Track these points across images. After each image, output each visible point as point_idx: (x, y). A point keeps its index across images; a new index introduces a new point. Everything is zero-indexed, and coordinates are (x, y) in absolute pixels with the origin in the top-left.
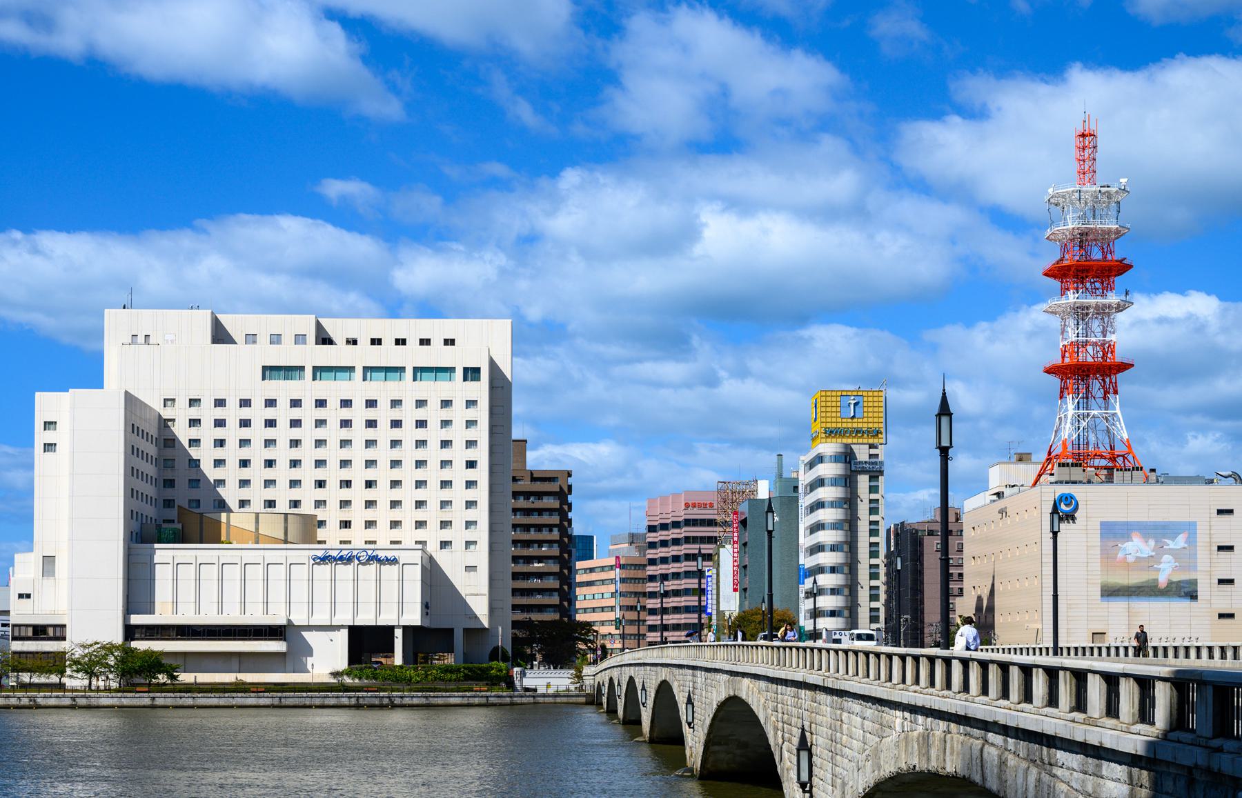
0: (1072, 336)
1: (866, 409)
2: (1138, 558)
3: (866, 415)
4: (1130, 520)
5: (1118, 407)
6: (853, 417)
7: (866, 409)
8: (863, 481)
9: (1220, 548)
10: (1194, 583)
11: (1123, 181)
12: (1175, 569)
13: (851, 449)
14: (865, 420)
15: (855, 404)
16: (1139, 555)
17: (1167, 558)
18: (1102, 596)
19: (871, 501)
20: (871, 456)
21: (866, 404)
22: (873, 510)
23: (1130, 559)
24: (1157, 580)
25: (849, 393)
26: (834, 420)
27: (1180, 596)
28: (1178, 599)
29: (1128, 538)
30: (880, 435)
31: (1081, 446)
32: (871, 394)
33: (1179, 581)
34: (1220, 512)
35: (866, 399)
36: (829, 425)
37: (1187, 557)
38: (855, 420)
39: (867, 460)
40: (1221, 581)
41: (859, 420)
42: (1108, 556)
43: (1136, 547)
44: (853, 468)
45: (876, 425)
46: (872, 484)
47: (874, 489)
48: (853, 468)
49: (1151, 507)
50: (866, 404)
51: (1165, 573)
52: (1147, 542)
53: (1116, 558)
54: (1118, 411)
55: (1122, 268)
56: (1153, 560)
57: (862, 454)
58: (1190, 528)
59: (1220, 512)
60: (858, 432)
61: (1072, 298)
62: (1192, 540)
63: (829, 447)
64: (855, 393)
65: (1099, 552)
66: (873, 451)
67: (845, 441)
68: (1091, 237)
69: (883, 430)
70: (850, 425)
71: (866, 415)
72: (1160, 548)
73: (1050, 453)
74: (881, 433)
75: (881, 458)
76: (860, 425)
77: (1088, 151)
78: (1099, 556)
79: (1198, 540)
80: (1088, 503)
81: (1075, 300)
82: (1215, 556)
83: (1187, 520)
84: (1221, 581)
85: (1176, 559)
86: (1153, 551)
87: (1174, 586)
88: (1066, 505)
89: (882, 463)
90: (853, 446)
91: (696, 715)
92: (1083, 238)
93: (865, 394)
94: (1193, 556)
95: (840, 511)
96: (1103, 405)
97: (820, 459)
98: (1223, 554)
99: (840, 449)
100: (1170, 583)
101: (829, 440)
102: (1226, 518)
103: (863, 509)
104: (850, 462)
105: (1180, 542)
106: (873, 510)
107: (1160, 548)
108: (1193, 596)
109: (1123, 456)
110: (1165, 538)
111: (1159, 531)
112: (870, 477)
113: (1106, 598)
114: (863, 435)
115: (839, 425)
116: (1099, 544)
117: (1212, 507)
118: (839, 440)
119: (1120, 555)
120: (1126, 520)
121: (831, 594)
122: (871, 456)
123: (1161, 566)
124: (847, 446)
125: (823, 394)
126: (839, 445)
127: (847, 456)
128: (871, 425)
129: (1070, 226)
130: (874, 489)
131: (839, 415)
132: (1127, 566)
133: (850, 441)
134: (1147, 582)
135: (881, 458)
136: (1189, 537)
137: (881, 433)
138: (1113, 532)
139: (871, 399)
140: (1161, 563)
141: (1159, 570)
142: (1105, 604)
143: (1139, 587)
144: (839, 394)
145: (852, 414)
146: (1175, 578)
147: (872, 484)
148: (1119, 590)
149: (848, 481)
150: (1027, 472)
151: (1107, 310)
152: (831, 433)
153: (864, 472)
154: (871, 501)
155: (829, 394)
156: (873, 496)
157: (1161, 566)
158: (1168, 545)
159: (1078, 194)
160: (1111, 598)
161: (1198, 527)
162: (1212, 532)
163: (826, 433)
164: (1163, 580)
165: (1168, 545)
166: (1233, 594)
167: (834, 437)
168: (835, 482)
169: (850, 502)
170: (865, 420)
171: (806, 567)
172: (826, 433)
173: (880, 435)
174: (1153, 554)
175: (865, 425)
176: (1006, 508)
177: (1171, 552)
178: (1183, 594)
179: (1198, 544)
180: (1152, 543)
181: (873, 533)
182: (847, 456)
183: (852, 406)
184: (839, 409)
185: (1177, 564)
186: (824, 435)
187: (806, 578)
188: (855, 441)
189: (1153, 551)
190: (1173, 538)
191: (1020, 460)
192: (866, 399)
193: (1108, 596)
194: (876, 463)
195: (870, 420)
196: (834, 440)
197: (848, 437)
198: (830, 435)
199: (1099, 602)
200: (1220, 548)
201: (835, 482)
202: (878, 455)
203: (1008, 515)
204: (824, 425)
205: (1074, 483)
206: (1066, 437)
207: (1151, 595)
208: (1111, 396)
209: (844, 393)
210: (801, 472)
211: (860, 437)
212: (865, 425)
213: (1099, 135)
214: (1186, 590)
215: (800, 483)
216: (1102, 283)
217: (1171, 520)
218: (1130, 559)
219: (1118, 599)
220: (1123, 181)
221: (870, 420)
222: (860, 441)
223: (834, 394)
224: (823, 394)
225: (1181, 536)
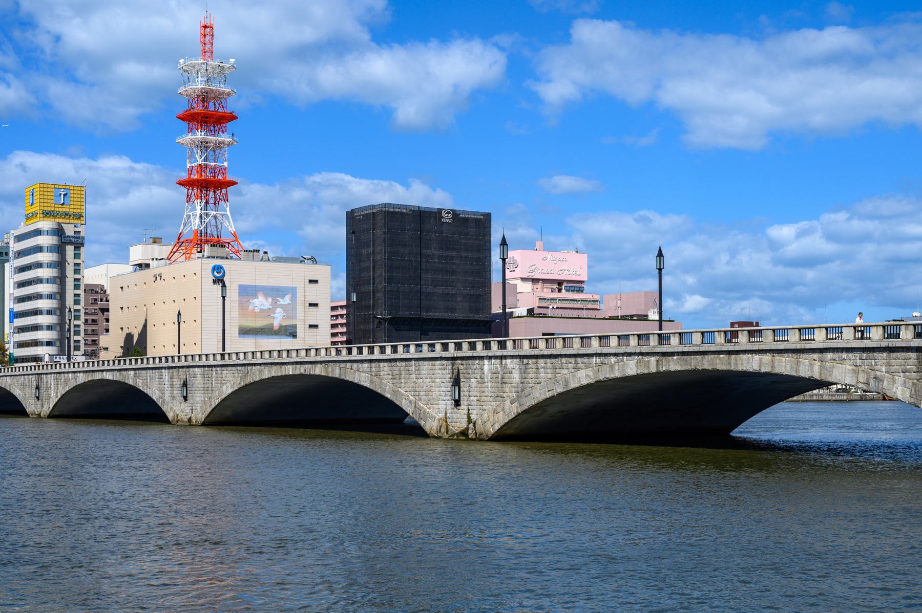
0: (200, 162)
1: (72, 199)
2: (261, 309)
3: (72, 203)
4: (257, 284)
5: (228, 209)
6: (63, 204)
7: (72, 199)
8: (70, 249)
9: (311, 305)
10: (295, 326)
11: (232, 60)
12: (284, 318)
13: (62, 226)
14: (72, 206)
15: (65, 195)
16: (262, 307)
17: (279, 310)
18: (239, 334)
19: (75, 264)
20: (75, 232)
21: (72, 195)
22: (77, 271)
23: (257, 310)
24: (273, 324)
25: (60, 187)
26: (49, 205)
27: (286, 335)
28: (285, 337)
29: (255, 296)
30: (82, 218)
31: (203, 235)
32: (75, 188)
33: (286, 326)
34: (311, 281)
35: (72, 192)
36: (45, 208)
37: (290, 311)
38: (64, 206)
39: (73, 235)
40: (311, 326)
41: (67, 207)
42: (243, 307)
43: (260, 302)
44: (63, 240)
45: (79, 211)
46: (76, 252)
47: (77, 256)
48: (63, 240)
49: (270, 276)
50: (72, 195)
51: (278, 320)
52: (267, 299)
53: (248, 309)
54: (228, 213)
55: (232, 117)
56: (271, 311)
57: (69, 231)
58: (293, 291)
59: (311, 281)
60: (66, 215)
61: (200, 135)
62: (294, 299)
63: (46, 224)
64: (64, 187)
65: (238, 305)
66: (76, 229)
67: (57, 220)
68: (212, 95)
69: (84, 215)
70: (60, 209)
71: (72, 203)
72: (275, 304)
73: (179, 239)
74: (82, 217)
75: (82, 234)
76: (68, 210)
77: (208, 38)
78: (238, 308)
79: (298, 299)
80: (232, 272)
81: (202, 136)
82: (307, 310)
83: (291, 286)
84: (311, 326)
85: (284, 311)
86: (271, 305)
87: (283, 328)
88: (217, 272)
89: (83, 238)
90: (62, 224)
91: (462, 394)
92: (205, 97)
93: (71, 188)
94: (294, 309)
95: (55, 270)
96: (214, 209)
97: (38, 232)
98: (312, 308)
99: (55, 226)
100: (281, 327)
101: (45, 219)
102: (313, 285)
103: (70, 269)
104: (61, 236)
105: (287, 300)
106: (77, 271)
107: (275, 304)
108: (294, 336)
109: (229, 243)
110: (278, 297)
111: (275, 292)
112: (75, 248)
113: (242, 336)
114: (70, 217)
115: (53, 209)
116: (238, 299)
117: (306, 278)
118: (53, 220)
119: (251, 307)
120: (254, 284)
121: (47, 330)
122: (75, 232)
123: (275, 315)
124: (59, 224)
125: (42, 185)
126: (54, 223)
127: (59, 232)
128: (75, 211)
129: (199, 87)
130: (77, 256)
131: (53, 201)
132: (254, 315)
133: (60, 221)
134: (266, 325)
135: (82, 234)
136: (292, 297)
137: (82, 217)
138: (247, 292)
139: (75, 192)
140: (275, 313)
141: (274, 318)
142: (241, 340)
143: (262, 329)
144: (53, 186)
145: (62, 202)
146: (284, 324)
147: (76, 252)
148: (250, 330)
149: (59, 249)
150: (163, 250)
151: (222, 145)
152: (47, 214)
153: (71, 243)
154: (75, 264)
155: (45, 186)
156: (77, 261)
157: (275, 315)
158: (280, 302)
159: (205, 66)
160: (246, 336)
161: (298, 291)
162: (306, 294)
163: (43, 213)
164: (276, 324)
165: (280, 302)
166: (318, 334)
167: (48, 217)
168: (51, 249)
169: (60, 265)
170: (72, 206)
171: (15, 311)
172: (43, 213)
173: (82, 218)
174: (271, 307)
175: (72, 210)
176: (161, 274)
177: (281, 306)
178: (288, 334)
179: (298, 302)
180: (270, 300)
181: (77, 287)
182: (59, 232)
183: (62, 196)
184: (53, 198)
185: (285, 314)
186: (41, 215)
187: (15, 318)
188: (64, 221)
189: (271, 305)
190: (283, 297)
191: (155, 242)
192: (72, 192)
193: (243, 334)
194: (79, 238)
195: (75, 207)
196: (49, 219)
197: (59, 218)
198: (46, 216)
199: (238, 338)
200: (311, 305)
201: (51, 249)
202: (80, 232)
203: (162, 278)
204: (42, 208)
205: (222, 258)
206: (196, 227)
207: (269, 334)
208: (222, 203)
209: (57, 186)
210: (11, 242)
211: (67, 219)
212: (72, 210)
213: (215, 28)
214: (290, 331)
215: (11, 249)
216: (214, 127)
217: (281, 285)
218: (257, 310)
219: (248, 336)
220: (232, 60)
221: (75, 207)
222: (68, 221)
223: (49, 186)
224: (42, 185)
225: (287, 296)
